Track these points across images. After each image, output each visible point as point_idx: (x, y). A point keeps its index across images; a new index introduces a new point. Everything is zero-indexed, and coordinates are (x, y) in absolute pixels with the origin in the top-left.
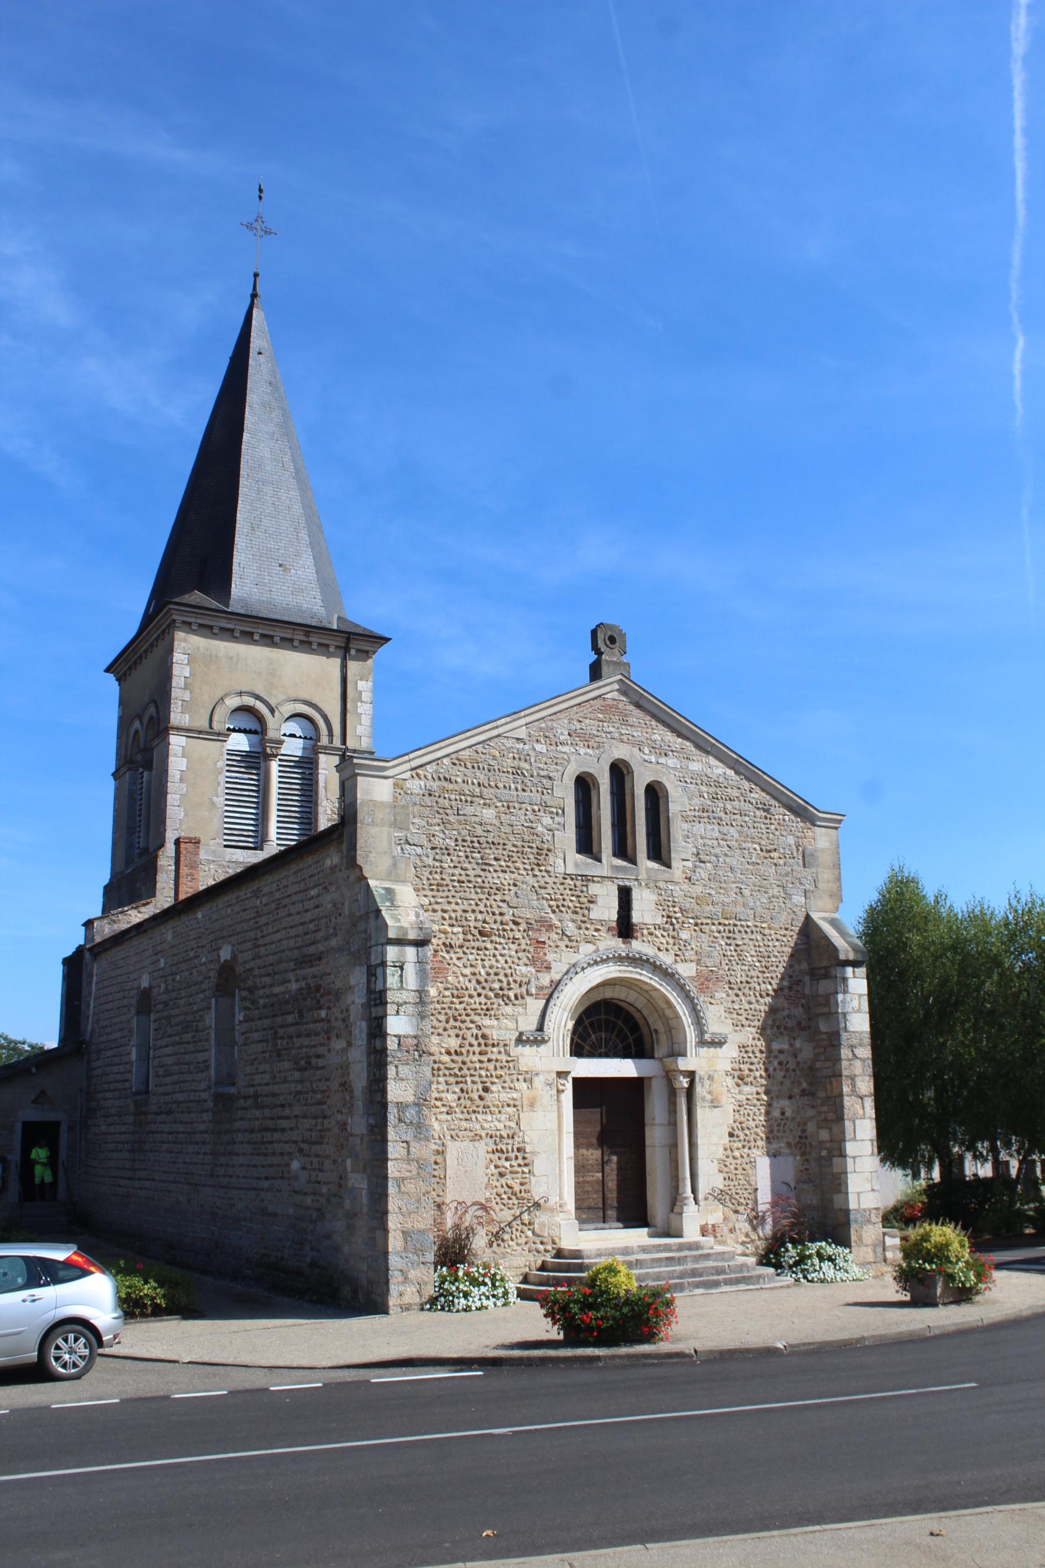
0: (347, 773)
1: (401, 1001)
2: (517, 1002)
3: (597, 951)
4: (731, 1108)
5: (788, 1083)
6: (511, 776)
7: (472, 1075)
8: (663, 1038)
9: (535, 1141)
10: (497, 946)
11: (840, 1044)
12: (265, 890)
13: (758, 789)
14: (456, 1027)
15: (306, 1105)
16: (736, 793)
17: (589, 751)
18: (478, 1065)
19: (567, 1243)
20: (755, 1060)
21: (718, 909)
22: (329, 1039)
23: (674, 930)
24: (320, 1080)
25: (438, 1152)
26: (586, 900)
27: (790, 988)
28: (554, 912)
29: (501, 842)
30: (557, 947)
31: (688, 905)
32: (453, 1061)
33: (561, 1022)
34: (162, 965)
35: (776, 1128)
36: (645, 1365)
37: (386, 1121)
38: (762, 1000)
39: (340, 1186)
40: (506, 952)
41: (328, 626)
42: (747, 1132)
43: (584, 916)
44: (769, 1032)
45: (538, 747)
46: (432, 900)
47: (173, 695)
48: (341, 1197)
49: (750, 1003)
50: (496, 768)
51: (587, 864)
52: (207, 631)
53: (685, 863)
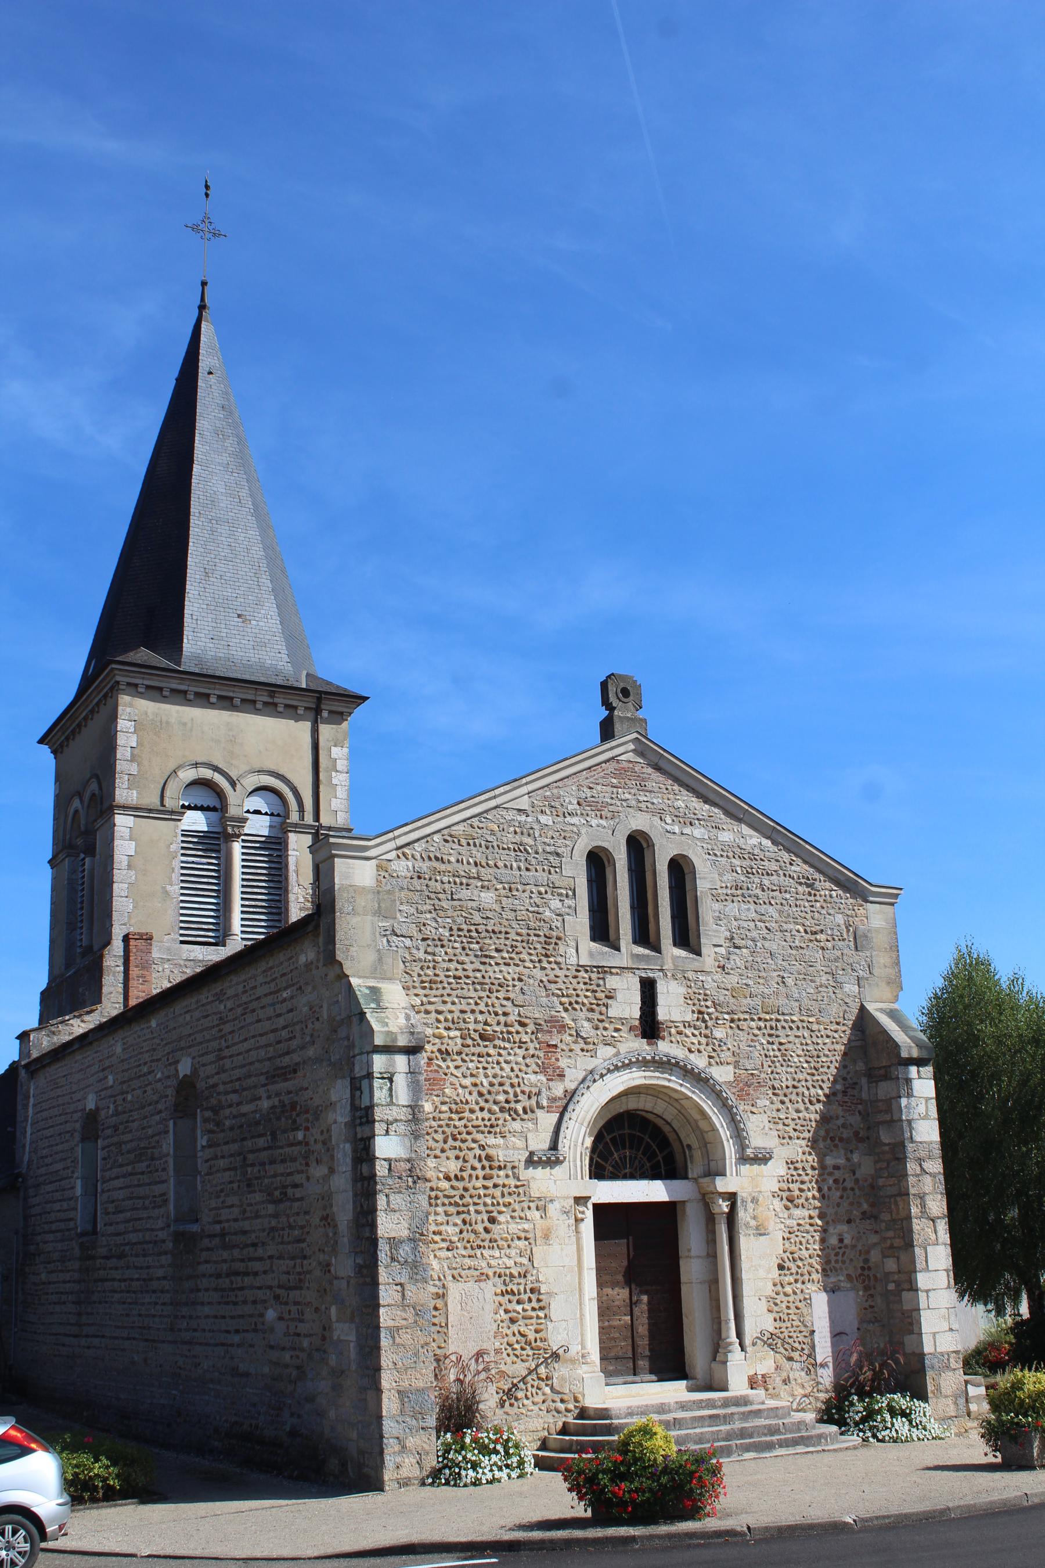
0: (323, 854)
1: (390, 1119)
2: (526, 1117)
3: (618, 1054)
4: (779, 1235)
5: (845, 1204)
6: (513, 854)
7: (475, 1204)
8: (697, 1154)
9: (551, 1280)
10: (501, 1051)
11: (906, 1157)
12: (230, 992)
13: (799, 861)
14: (455, 1148)
15: (282, 1243)
16: (773, 866)
17: (601, 821)
18: (482, 1192)
19: (593, 1401)
20: (806, 1178)
21: (758, 1001)
22: (307, 1165)
23: (706, 1027)
24: (298, 1214)
25: (438, 1296)
26: (603, 995)
27: (845, 1093)
28: (566, 1010)
29: (503, 930)
30: (571, 1050)
31: (722, 998)
32: (452, 1187)
33: (578, 1139)
34: (111, 1083)
35: (833, 1258)
36: (689, 1546)
37: (377, 1260)
38: (812, 1108)
39: (324, 1338)
40: (512, 1058)
41: (296, 684)
42: (800, 1263)
43: (601, 1014)
44: (821, 1145)
45: (543, 819)
46: (425, 999)
47: (118, 768)
48: (325, 1352)
49: (798, 1111)
50: (495, 844)
51: (603, 953)
52: (156, 694)
53: (717, 949)
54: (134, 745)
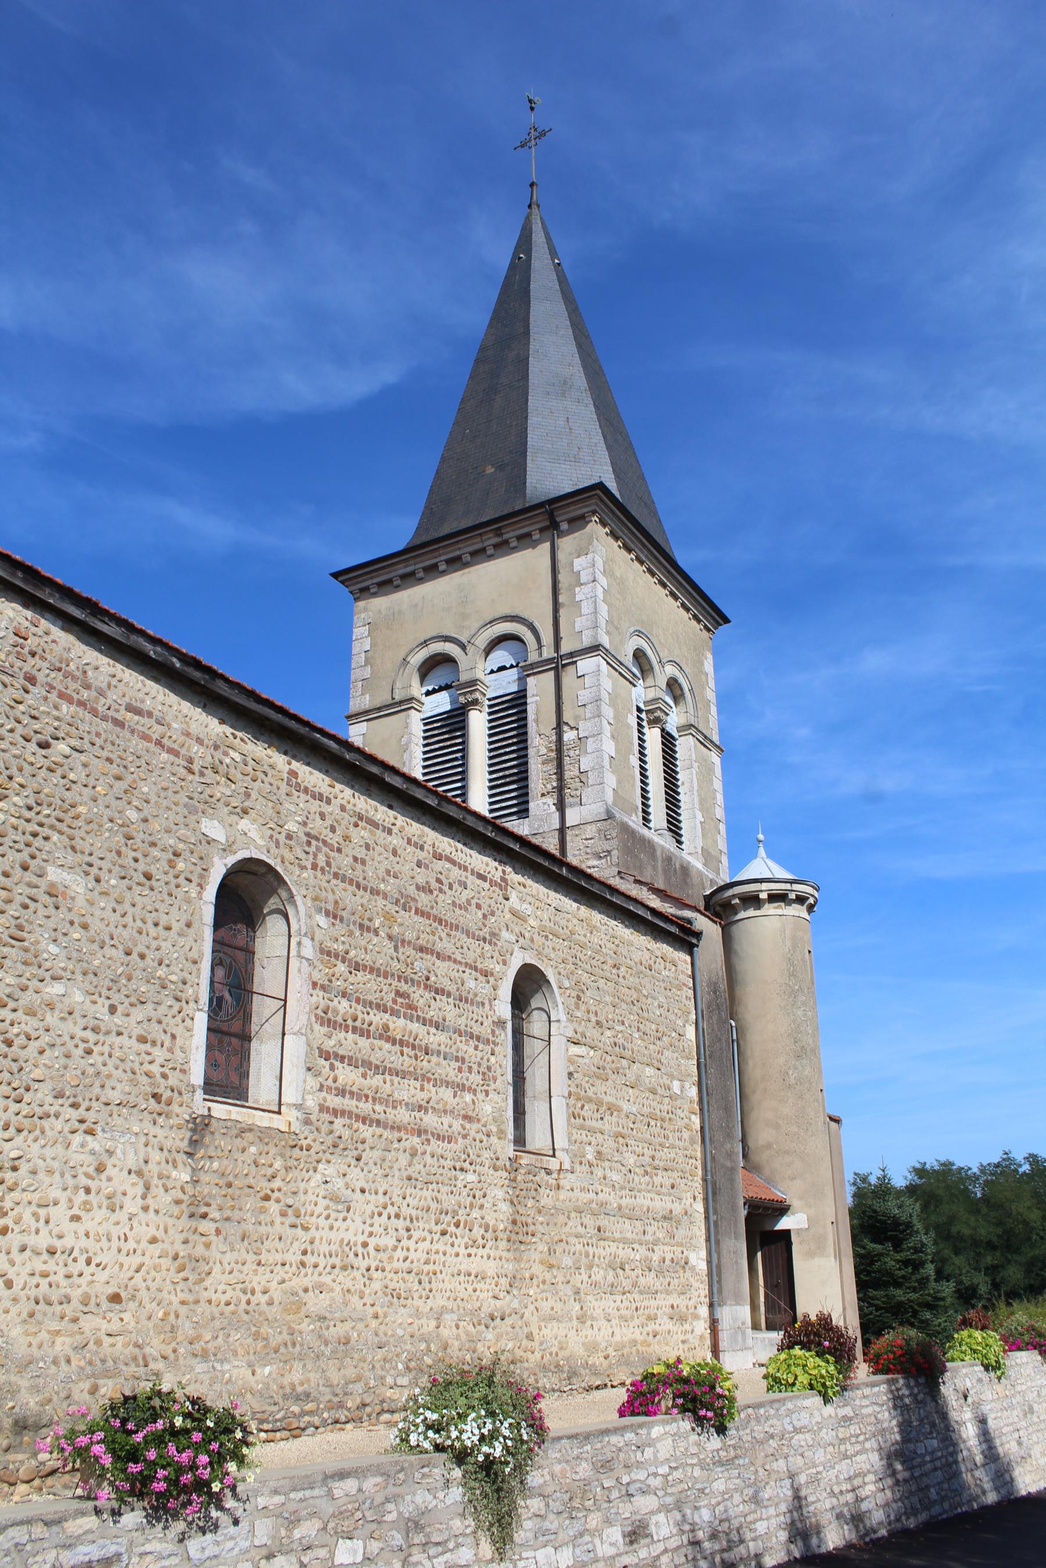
54: (368, 648)
